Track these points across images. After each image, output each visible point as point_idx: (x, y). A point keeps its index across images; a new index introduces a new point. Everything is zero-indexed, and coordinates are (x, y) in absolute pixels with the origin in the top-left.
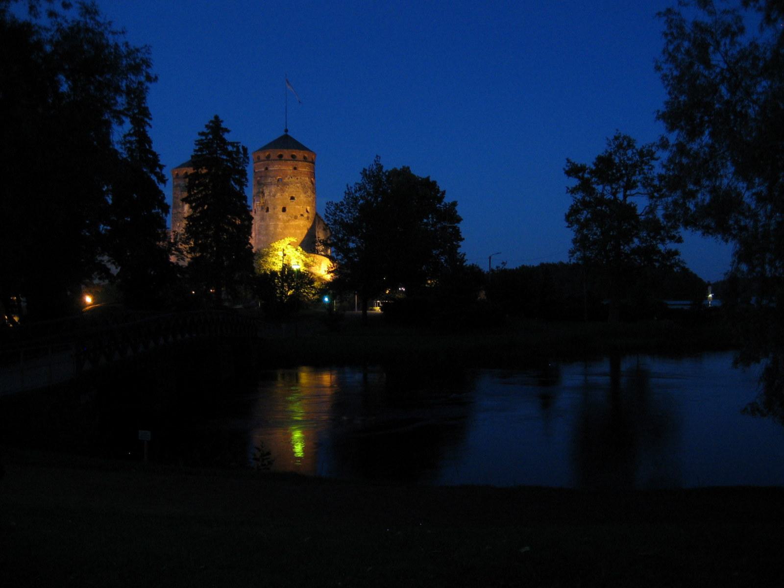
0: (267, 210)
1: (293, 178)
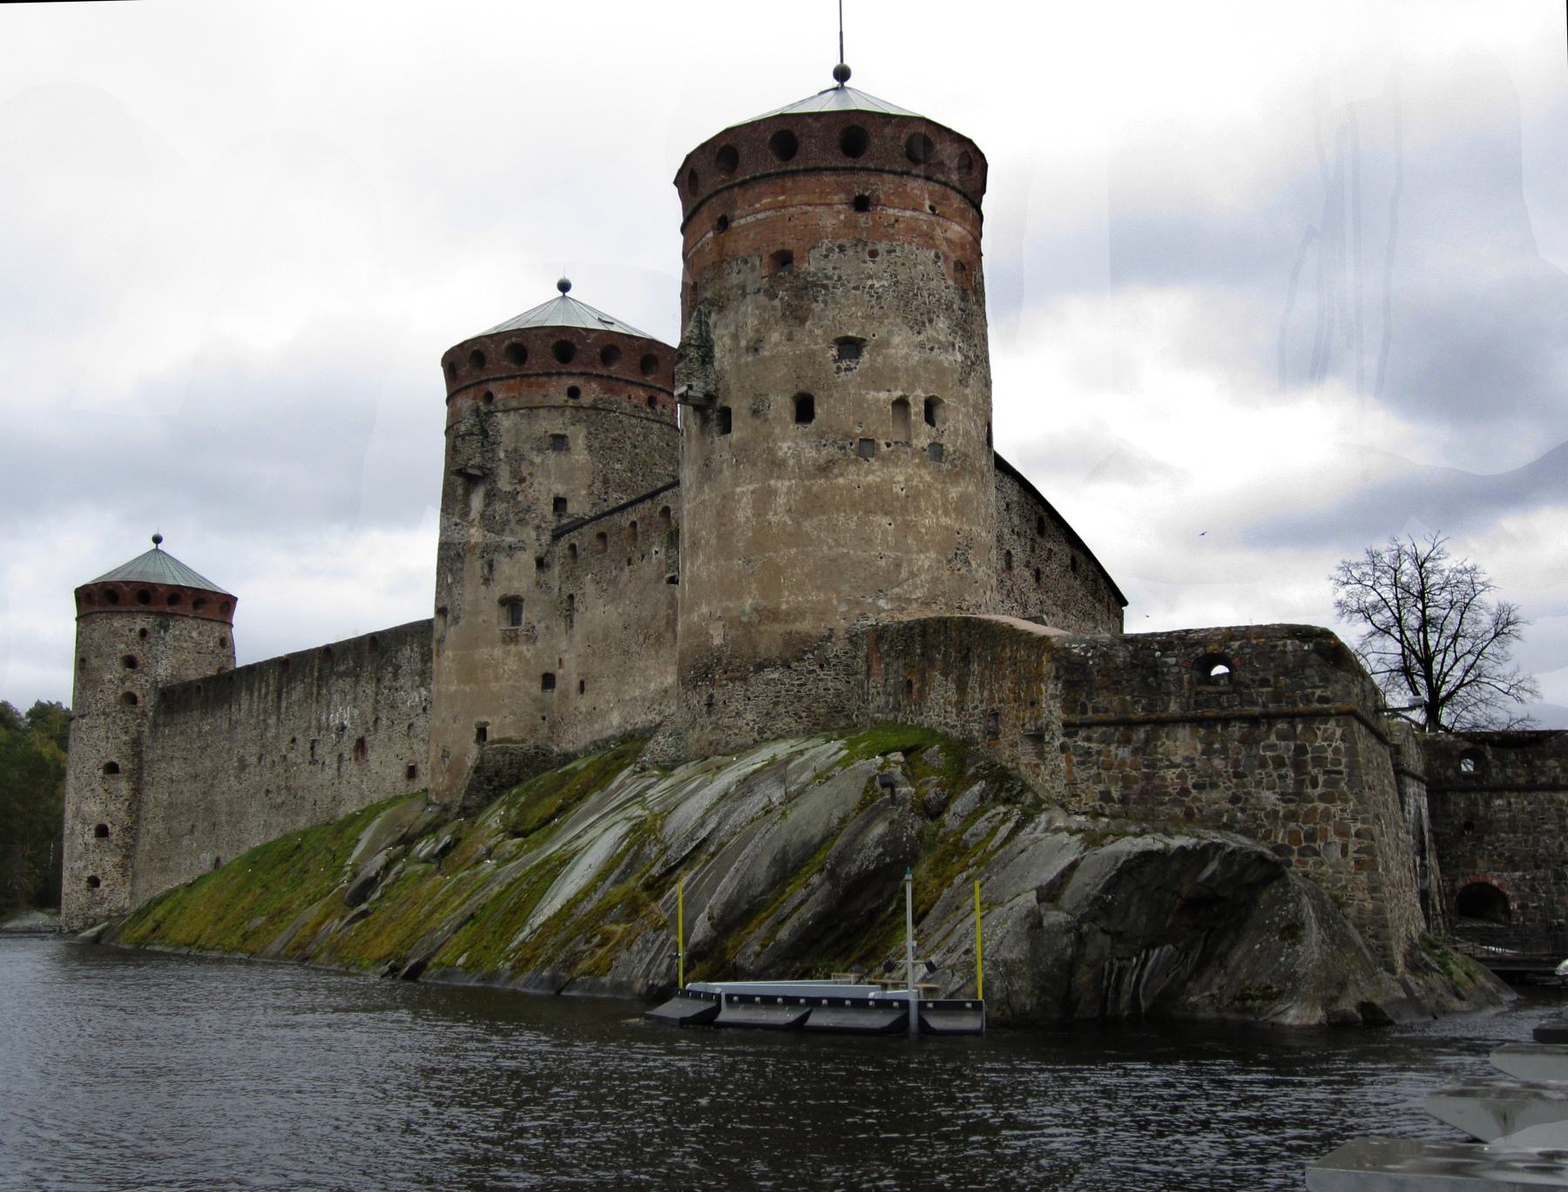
0: (726, 429)
1: (851, 253)
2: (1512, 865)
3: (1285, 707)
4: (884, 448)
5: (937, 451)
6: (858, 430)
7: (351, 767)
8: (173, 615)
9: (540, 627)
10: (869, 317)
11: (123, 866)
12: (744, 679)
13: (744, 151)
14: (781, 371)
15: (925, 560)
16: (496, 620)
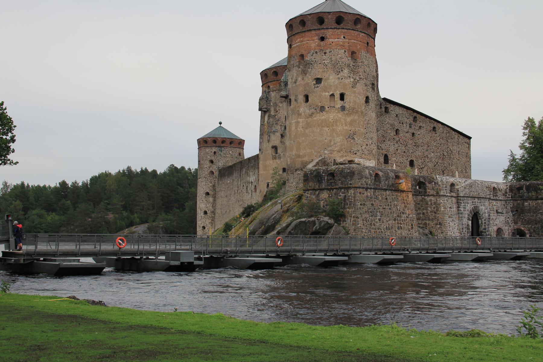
1: (319, 53)
2: (528, 223)
3: (344, 186)
4: (327, 109)
5: (343, 108)
6: (320, 104)
7: (254, 194)
8: (223, 147)
9: (282, 154)
10: (324, 71)
11: (211, 223)
12: (293, 173)
13: (294, 25)
14: (301, 89)
15: (338, 139)
16: (270, 151)
